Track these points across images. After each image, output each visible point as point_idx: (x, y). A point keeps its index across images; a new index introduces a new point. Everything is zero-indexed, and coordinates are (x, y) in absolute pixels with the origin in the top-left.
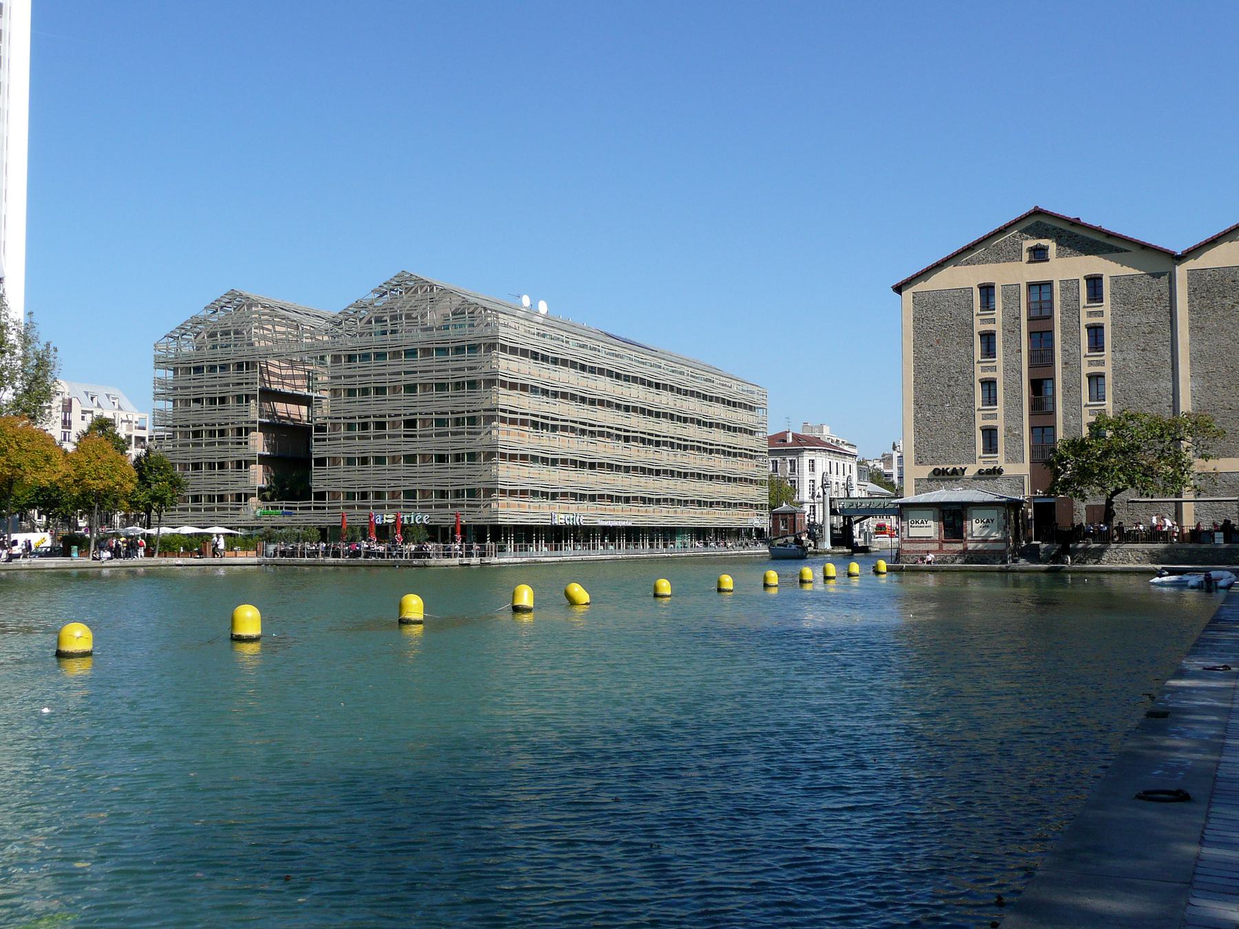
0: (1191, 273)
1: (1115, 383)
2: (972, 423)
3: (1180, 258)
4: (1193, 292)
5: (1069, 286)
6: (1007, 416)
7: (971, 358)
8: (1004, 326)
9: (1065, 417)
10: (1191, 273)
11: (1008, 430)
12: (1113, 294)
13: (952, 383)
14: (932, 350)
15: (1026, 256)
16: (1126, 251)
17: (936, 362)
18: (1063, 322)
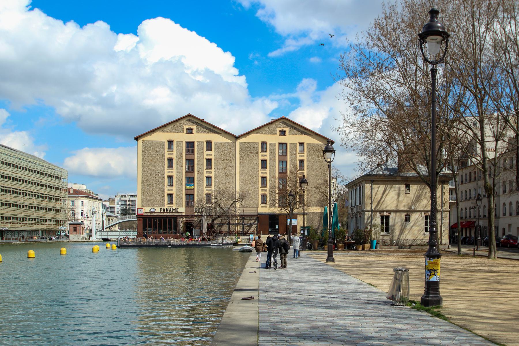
0: (241, 143)
1: (215, 180)
2: (163, 192)
3: (237, 138)
4: (241, 150)
5: (200, 143)
6: (176, 189)
7: (164, 168)
8: (176, 157)
9: (198, 191)
10: (241, 143)
11: (177, 195)
12: (215, 148)
13: (157, 176)
14: (149, 163)
15: (185, 131)
16: (220, 133)
17: (151, 168)
18: (198, 157)
